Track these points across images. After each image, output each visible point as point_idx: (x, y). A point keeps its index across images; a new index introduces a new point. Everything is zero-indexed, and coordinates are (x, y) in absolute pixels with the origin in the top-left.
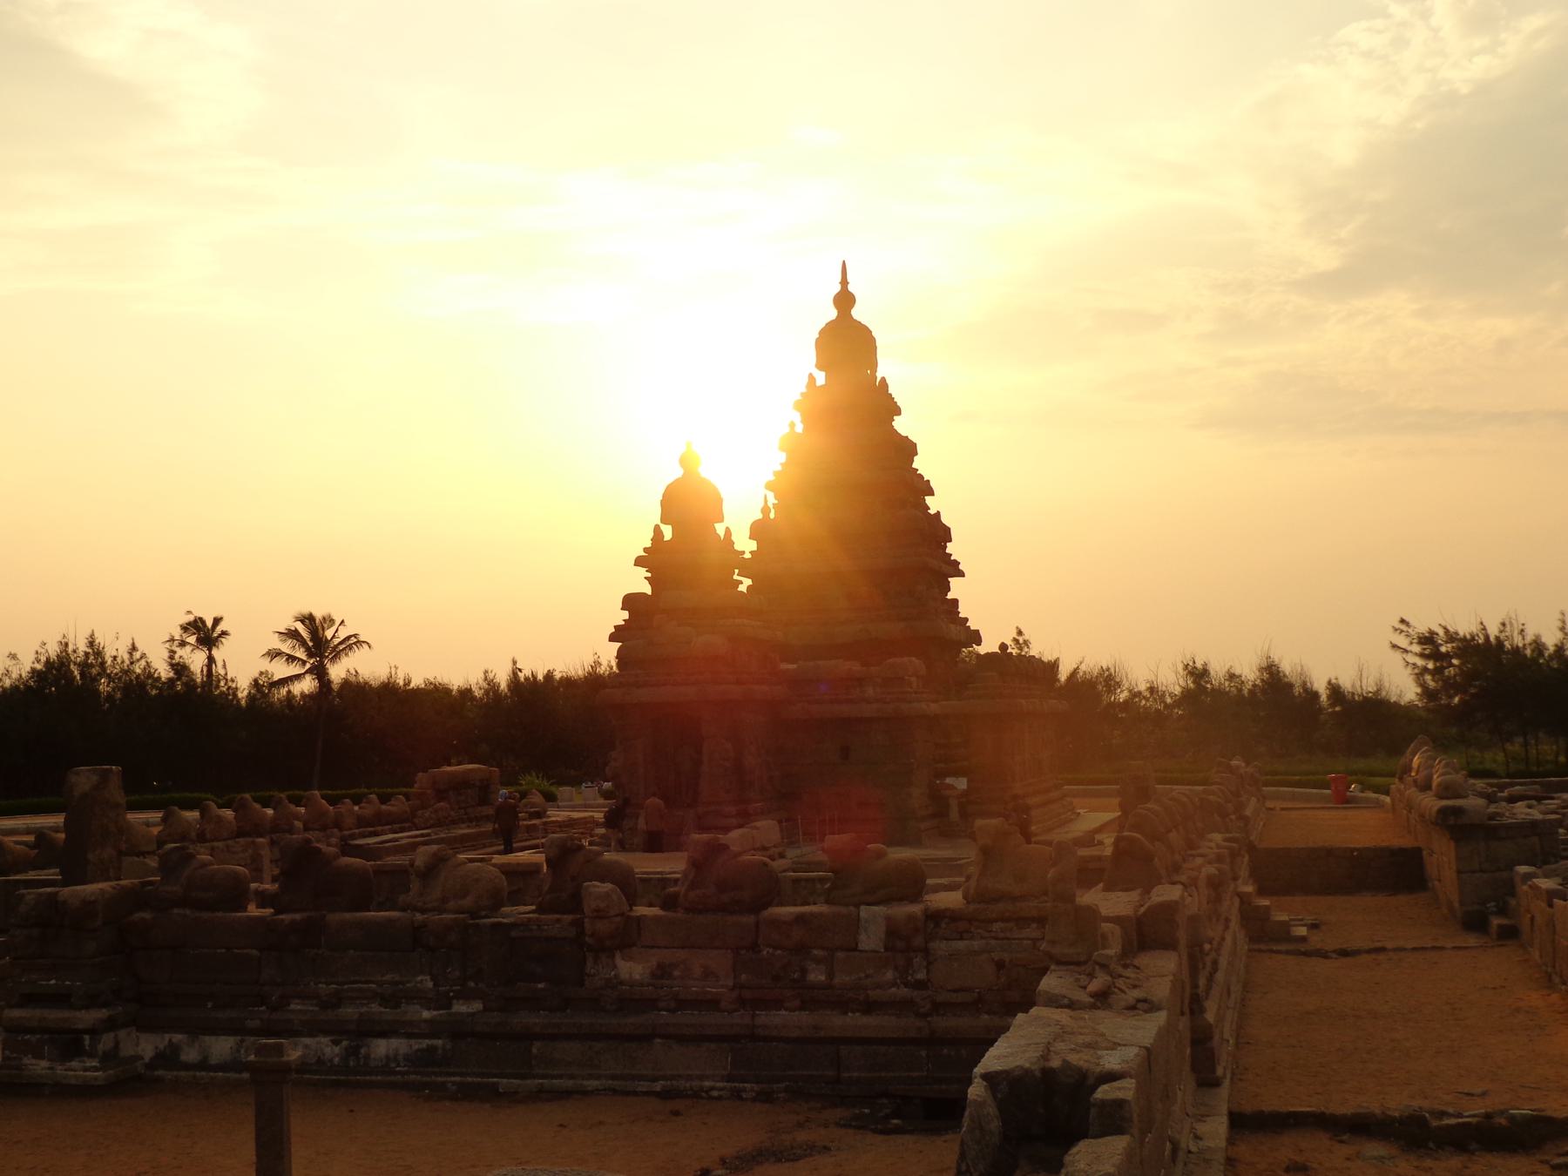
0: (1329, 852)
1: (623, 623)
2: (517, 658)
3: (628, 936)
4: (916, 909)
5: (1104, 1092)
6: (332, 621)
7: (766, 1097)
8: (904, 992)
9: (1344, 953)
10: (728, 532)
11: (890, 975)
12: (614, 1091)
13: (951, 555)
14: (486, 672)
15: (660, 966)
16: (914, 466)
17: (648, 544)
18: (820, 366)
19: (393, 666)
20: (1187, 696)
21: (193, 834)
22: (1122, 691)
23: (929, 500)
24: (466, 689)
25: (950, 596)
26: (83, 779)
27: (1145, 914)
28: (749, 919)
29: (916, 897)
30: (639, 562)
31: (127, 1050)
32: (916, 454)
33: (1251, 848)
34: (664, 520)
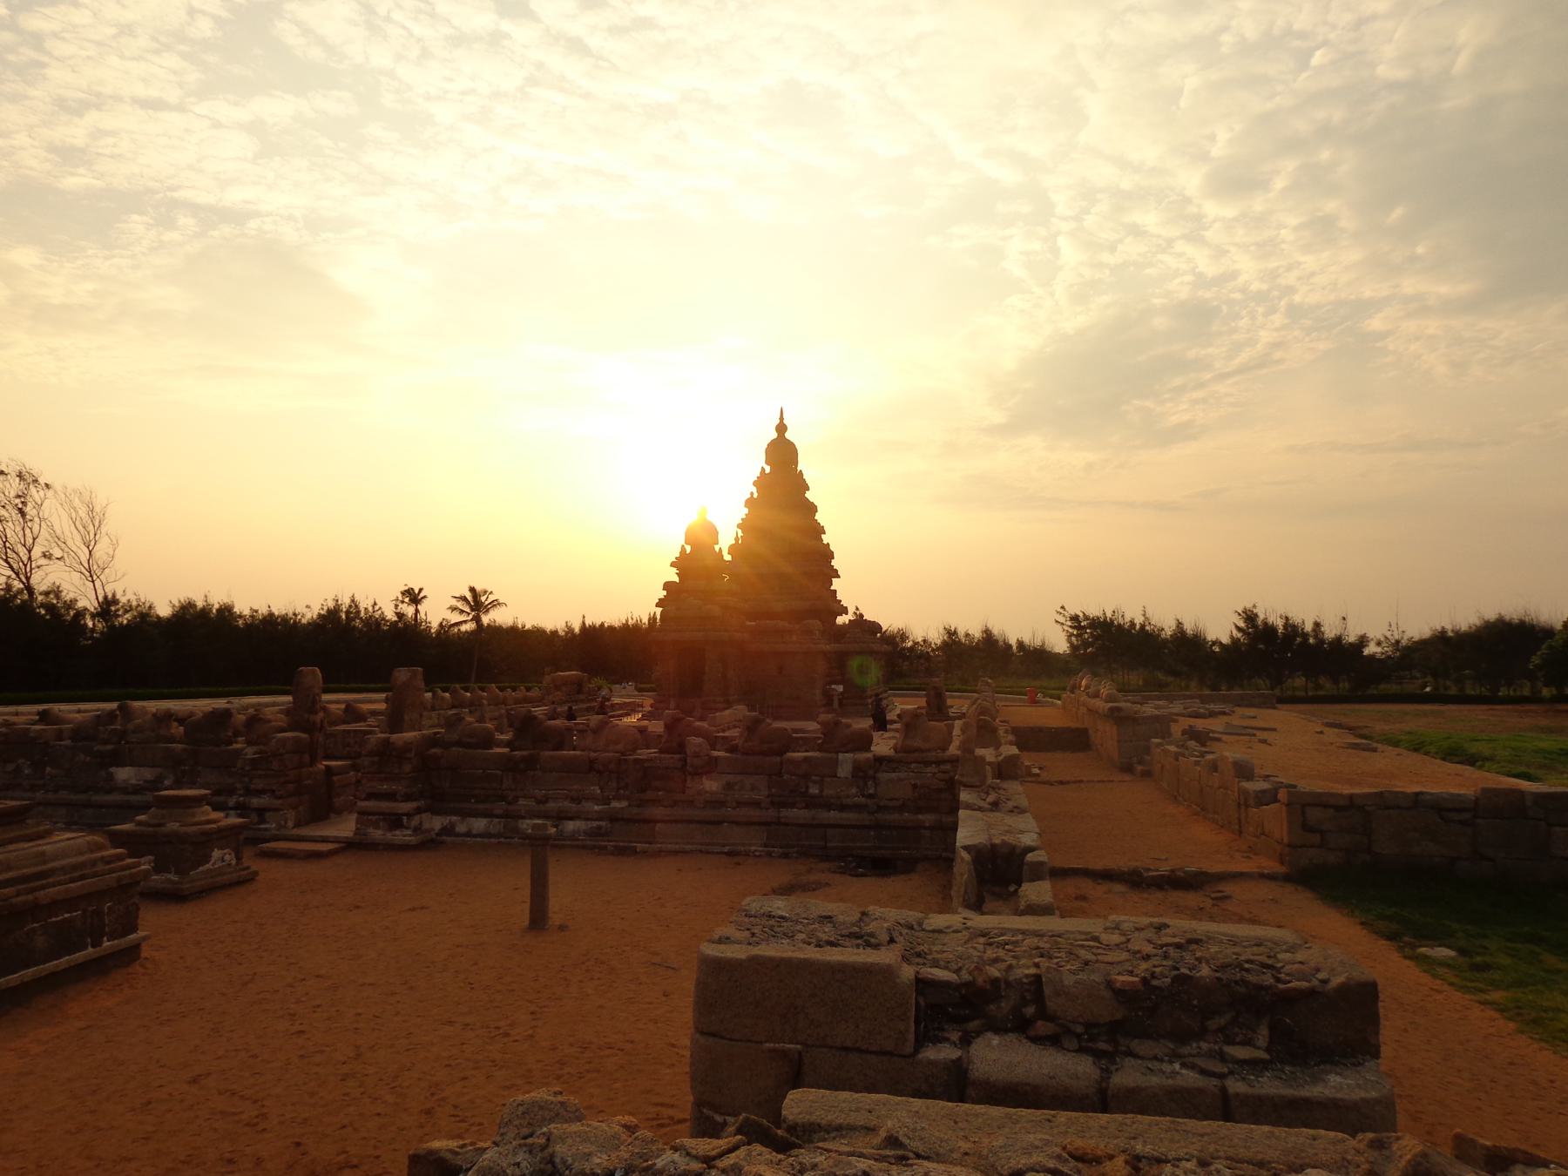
0: (1040, 730)
3: (711, 766)
4: (869, 755)
5: (1030, 857)
7: (786, 856)
8: (862, 800)
9: (1061, 783)
11: (854, 791)
12: (701, 851)
16: (816, 518)
20: (945, 643)
21: (429, 707)
23: (823, 536)
25: (832, 588)
26: (402, 675)
27: (1002, 761)
28: (778, 759)
30: (673, 564)
31: (426, 826)
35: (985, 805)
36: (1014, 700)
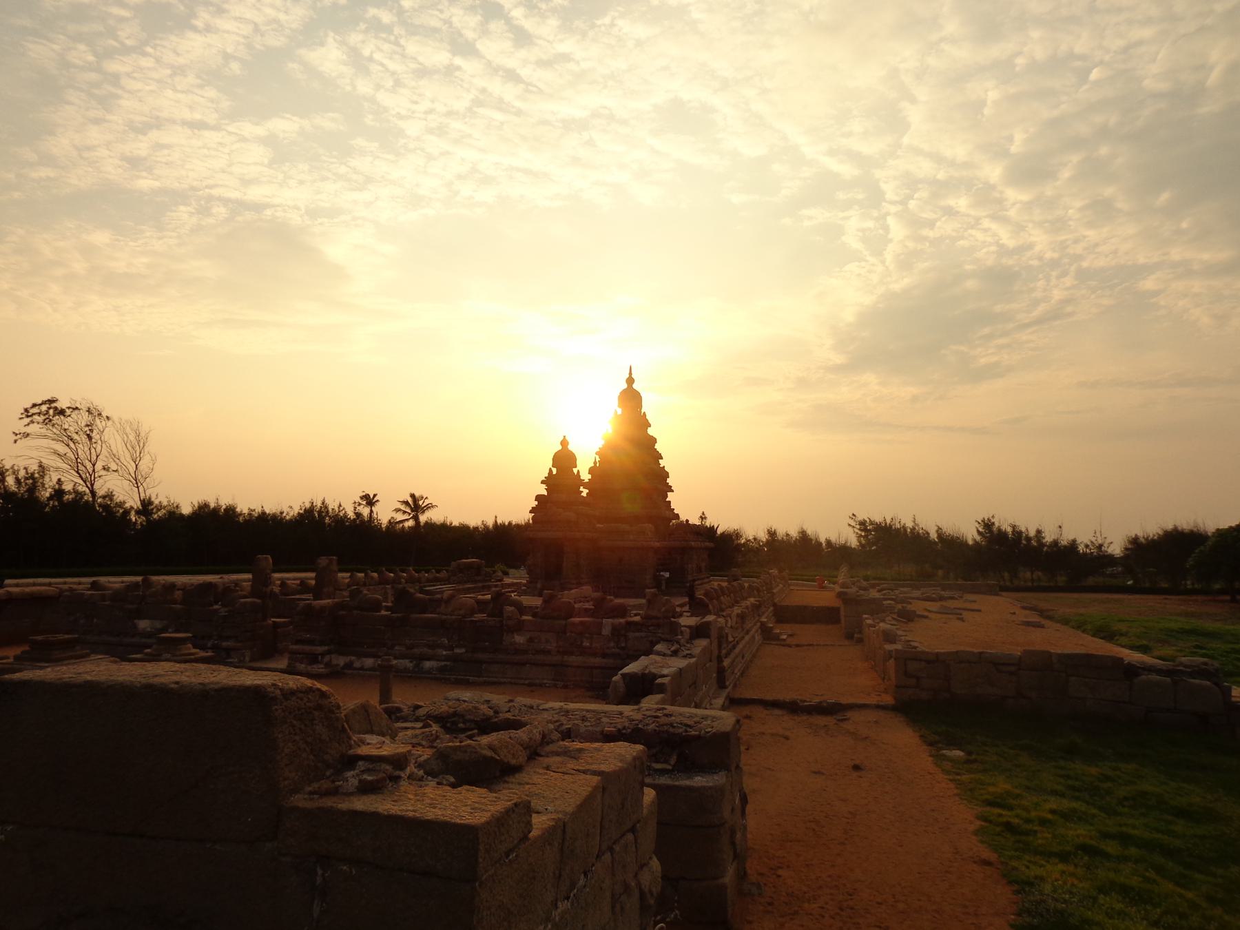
0: (805, 607)
2: (498, 516)
3: (519, 627)
4: (622, 621)
6: (423, 497)
7: (565, 687)
8: (617, 651)
9: (797, 646)
11: (612, 644)
12: (511, 683)
14: (483, 521)
15: (531, 638)
20: (768, 541)
21: (362, 583)
23: (660, 461)
25: (667, 500)
26: (323, 561)
28: (564, 622)
29: (623, 616)
30: (543, 482)
31: (334, 662)
33: (774, 605)
34: (553, 466)
35: (669, 652)
36: (803, 585)
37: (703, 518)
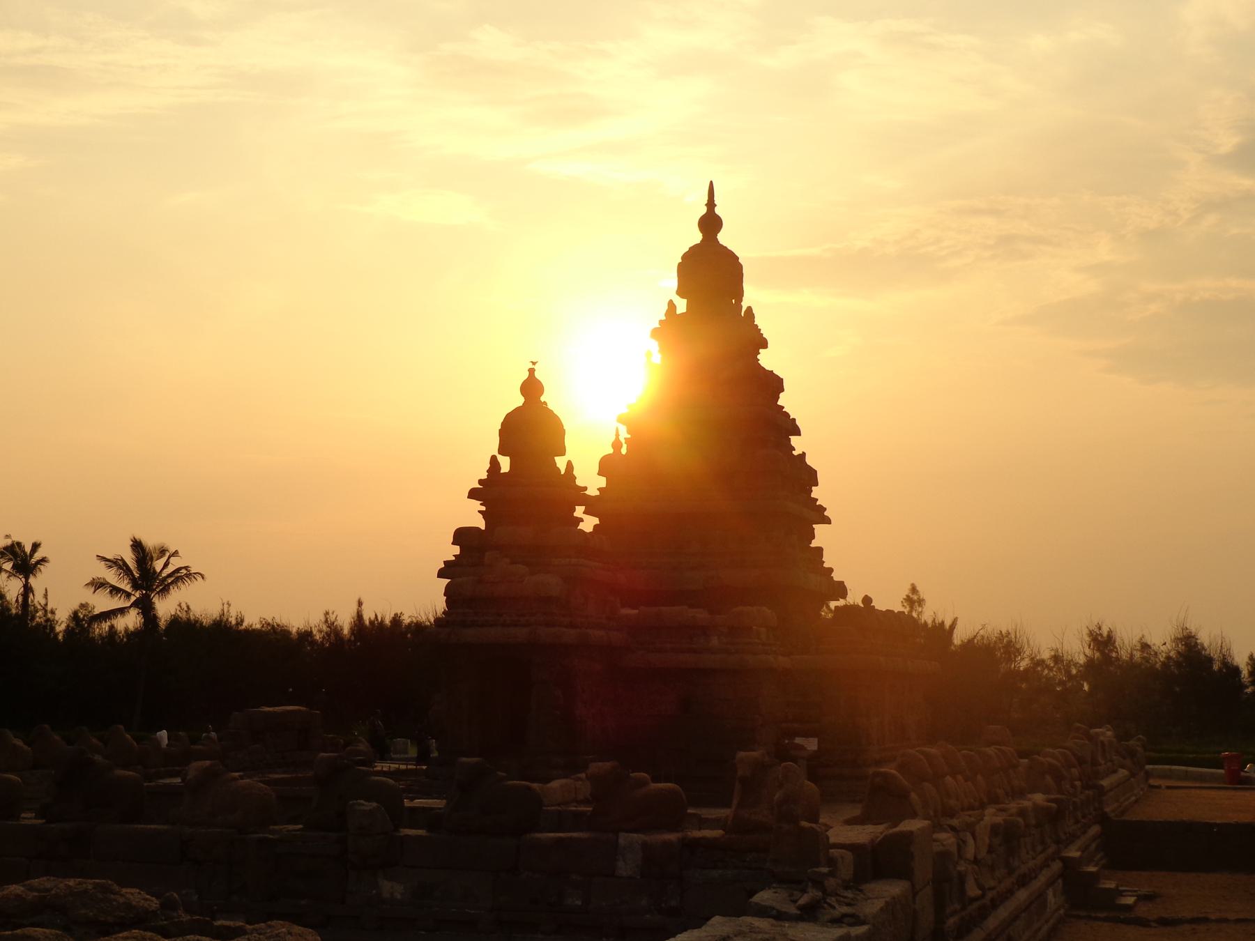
1: (454, 558)
2: (363, 600)
4: (672, 837)
9: (1164, 922)
10: (570, 466)
13: (817, 500)
14: (327, 613)
16: (780, 403)
17: (484, 476)
18: (681, 292)
19: (225, 601)
20: (1090, 663)
22: (1022, 659)
23: (794, 440)
24: (306, 631)
25: (814, 544)
30: (473, 494)
32: (783, 390)
33: (1103, 819)
35: (793, 910)
36: (1187, 776)
37: (914, 599)
